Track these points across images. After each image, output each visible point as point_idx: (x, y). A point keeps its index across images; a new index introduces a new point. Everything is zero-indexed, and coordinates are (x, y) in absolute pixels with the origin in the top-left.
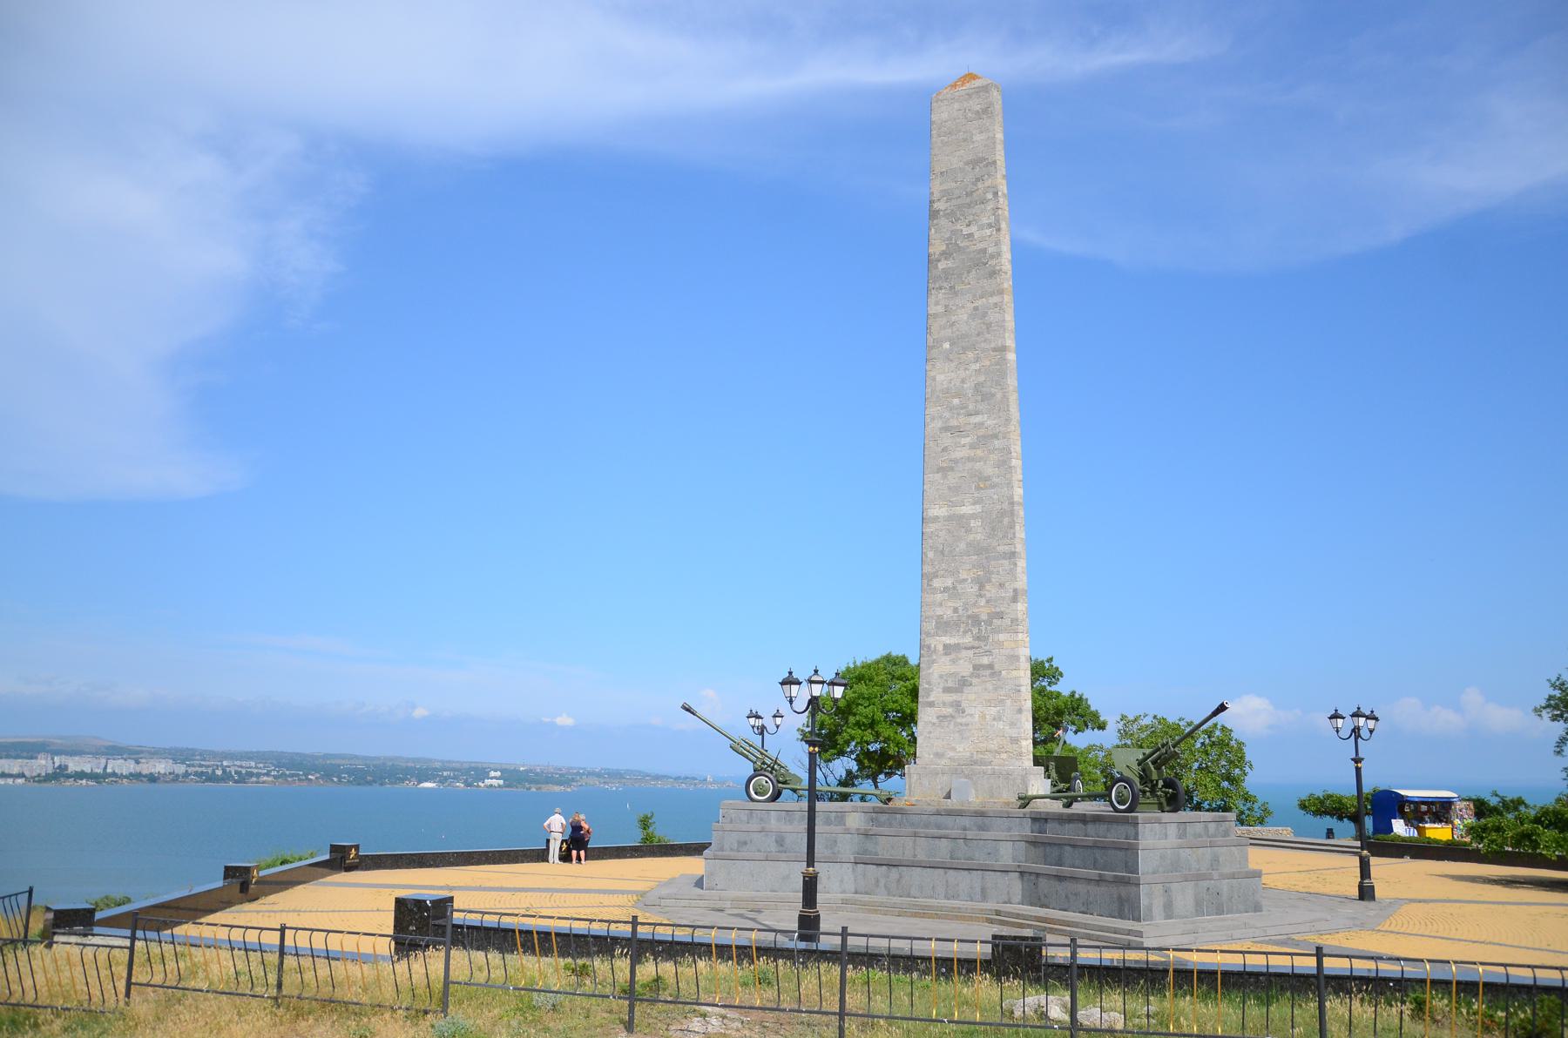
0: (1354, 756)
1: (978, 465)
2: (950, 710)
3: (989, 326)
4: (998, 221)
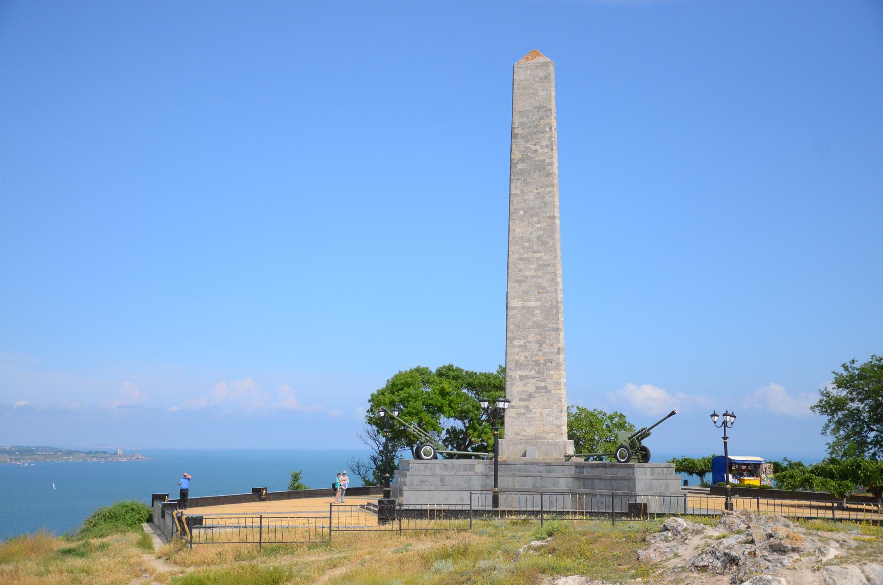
0: (723, 436)
1: (539, 280)
2: (523, 410)
3: (546, 204)
4: (552, 145)
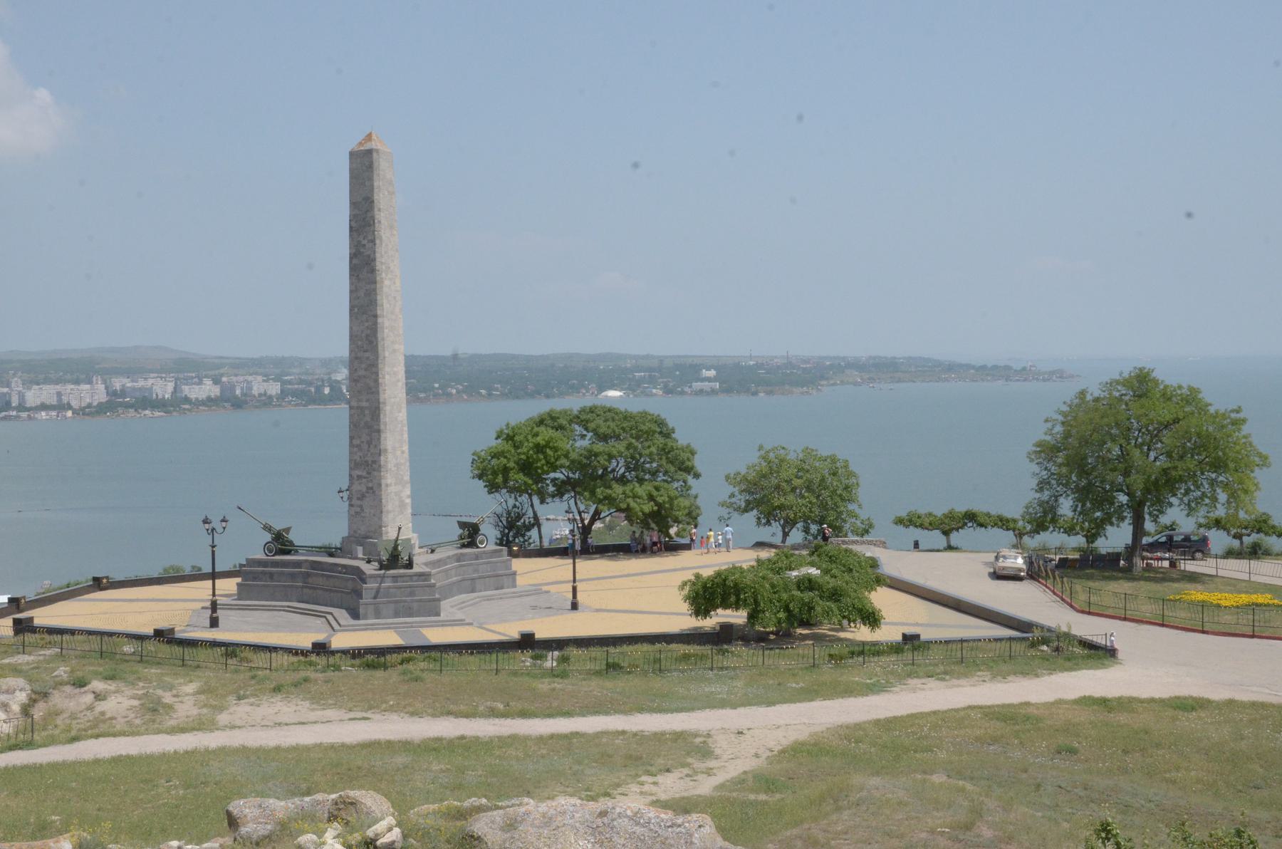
2: (358, 509)
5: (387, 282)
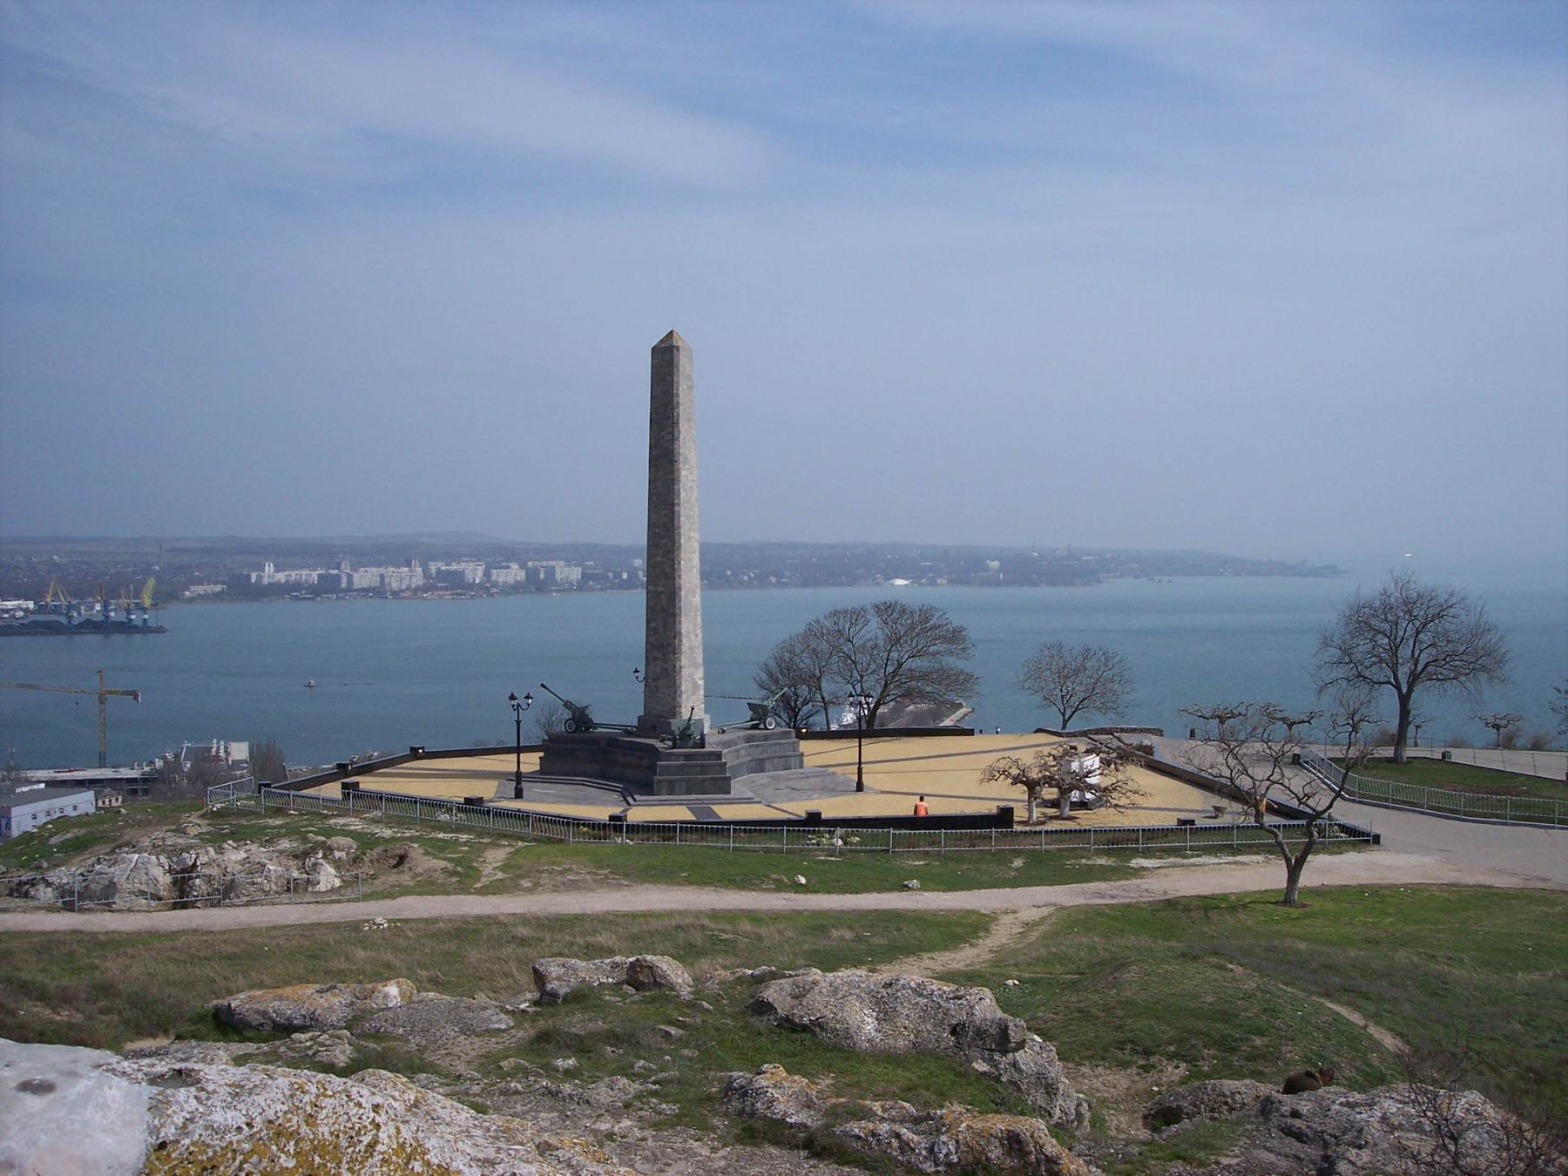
5: (683, 473)
